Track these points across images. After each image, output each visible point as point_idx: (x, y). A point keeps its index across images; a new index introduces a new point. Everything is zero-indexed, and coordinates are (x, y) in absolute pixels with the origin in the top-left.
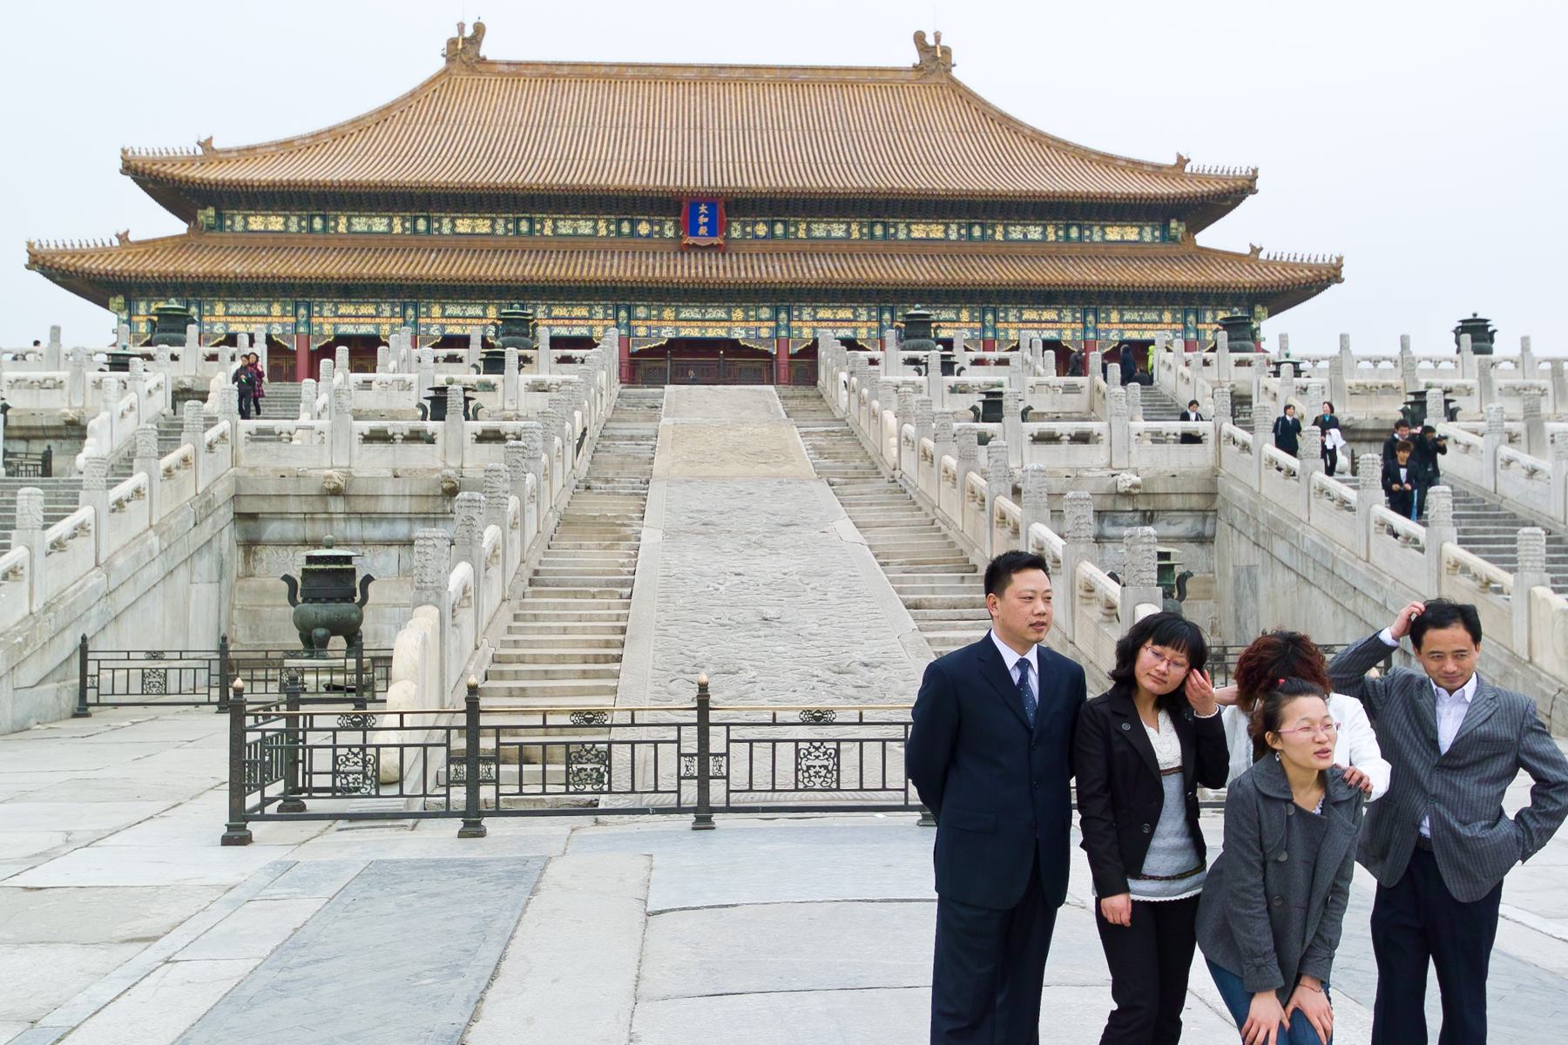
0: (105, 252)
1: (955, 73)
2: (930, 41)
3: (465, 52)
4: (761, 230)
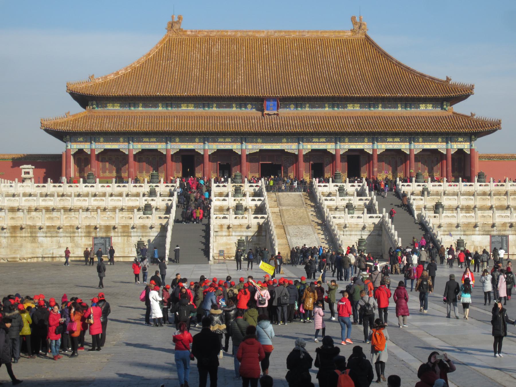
2: (357, 20)
4: (292, 106)
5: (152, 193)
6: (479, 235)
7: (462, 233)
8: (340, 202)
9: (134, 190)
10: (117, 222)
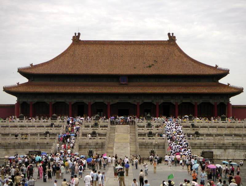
0: (14, 87)
1: (177, 42)
2: (171, 35)
3: (76, 39)
5: (52, 125)
6: (215, 149)
7: (207, 148)
8: (146, 131)
9: (44, 124)
10: (29, 141)
